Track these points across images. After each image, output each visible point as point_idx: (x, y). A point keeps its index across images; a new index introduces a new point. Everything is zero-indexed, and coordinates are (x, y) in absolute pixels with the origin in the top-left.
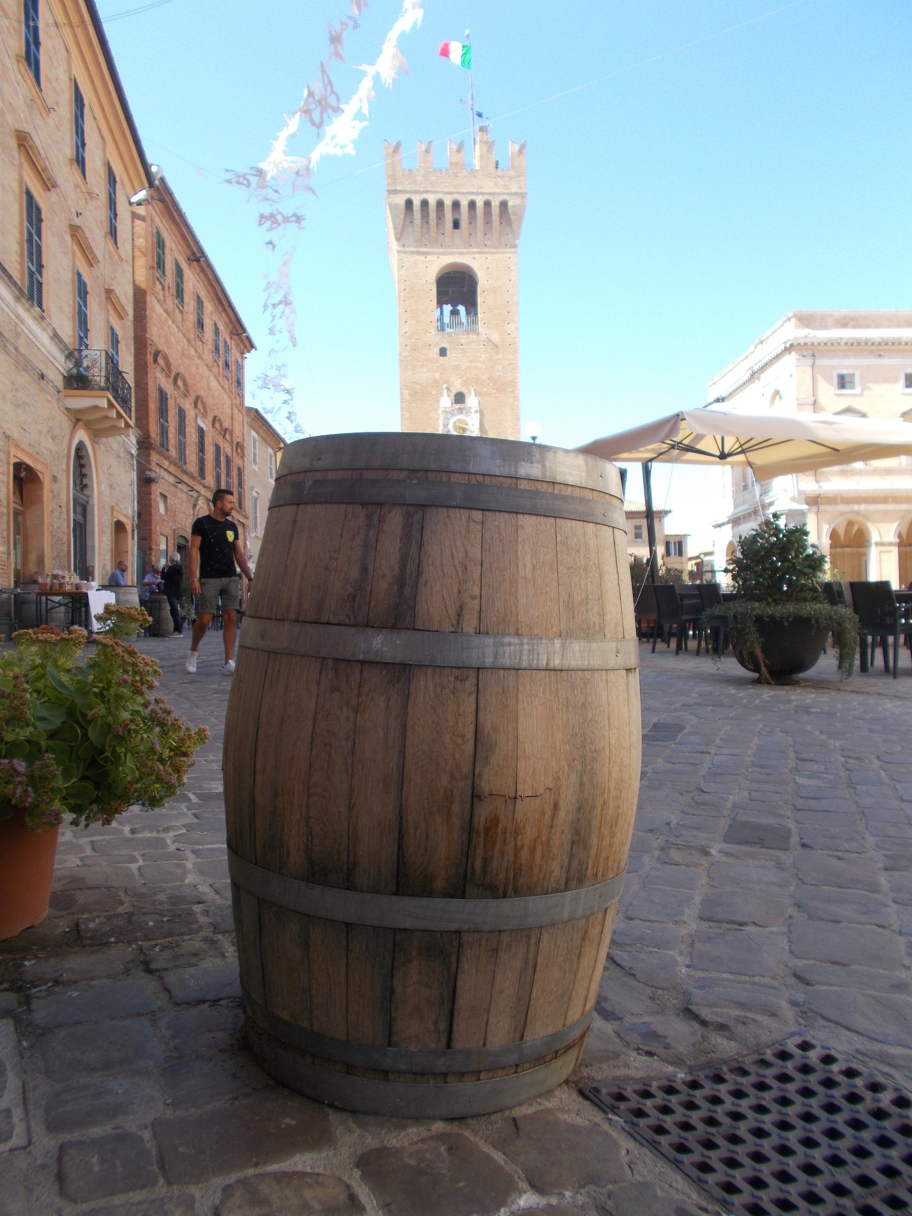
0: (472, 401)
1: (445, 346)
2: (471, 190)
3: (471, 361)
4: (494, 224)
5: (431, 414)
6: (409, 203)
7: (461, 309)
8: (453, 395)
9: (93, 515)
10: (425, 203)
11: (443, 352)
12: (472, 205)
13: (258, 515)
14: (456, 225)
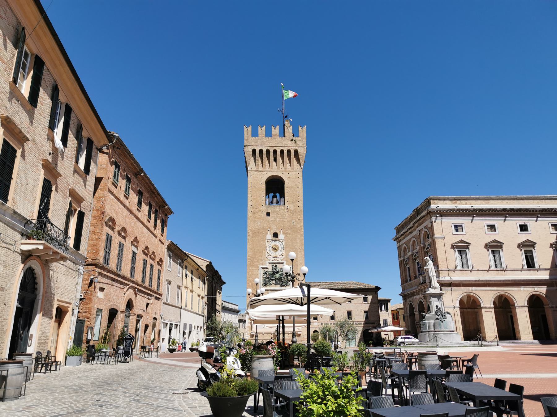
0: (281, 236)
1: (269, 211)
2: (281, 146)
3: (281, 219)
5: (262, 242)
6: (254, 151)
7: (278, 195)
8: (272, 234)
9: (38, 305)
10: (261, 151)
11: (268, 214)
12: (282, 152)
13: (169, 293)
14: (275, 160)
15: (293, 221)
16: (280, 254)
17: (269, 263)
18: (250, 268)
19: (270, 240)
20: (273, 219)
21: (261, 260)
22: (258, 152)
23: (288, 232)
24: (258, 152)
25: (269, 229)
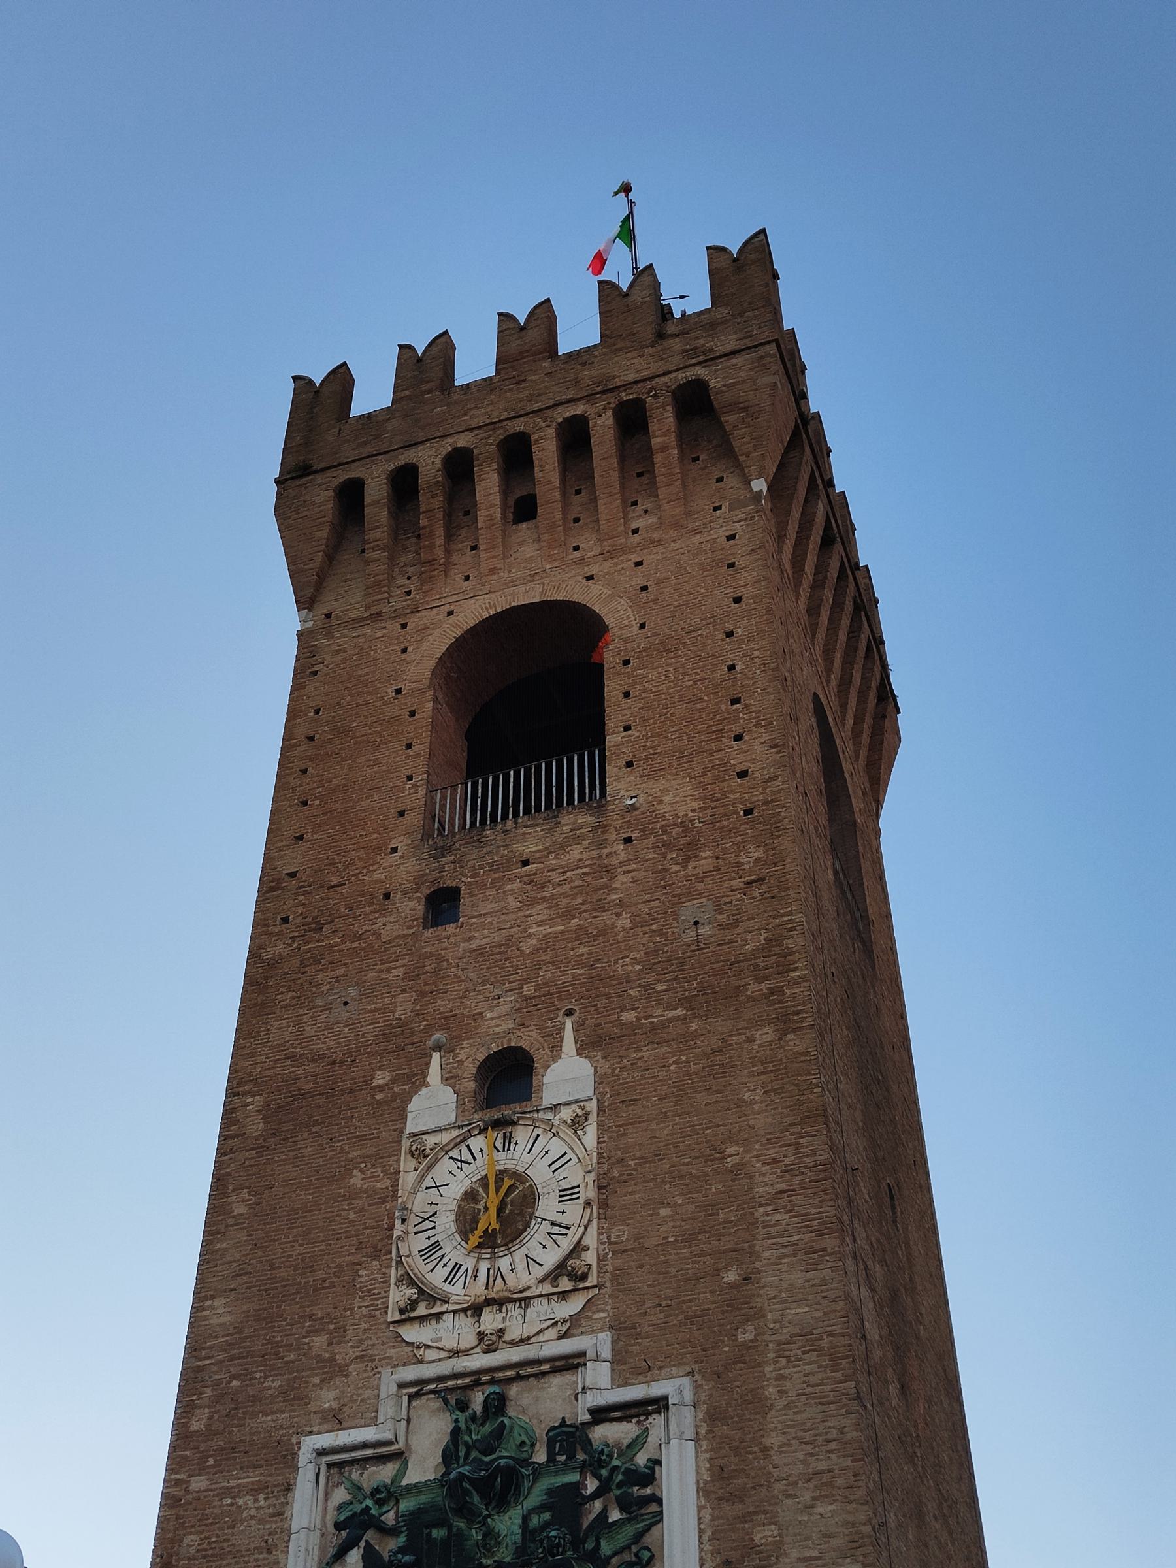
3: (568, 914)
4: (658, 458)
5: (357, 1180)
8: (471, 1068)
15: (688, 912)
16: (551, 1258)
17: (417, 1390)
18: (199, 1483)
19: (446, 1138)
20: (483, 939)
21: (333, 1370)
22: (376, 490)
23: (633, 1027)
24: (376, 490)
25: (439, 1036)
